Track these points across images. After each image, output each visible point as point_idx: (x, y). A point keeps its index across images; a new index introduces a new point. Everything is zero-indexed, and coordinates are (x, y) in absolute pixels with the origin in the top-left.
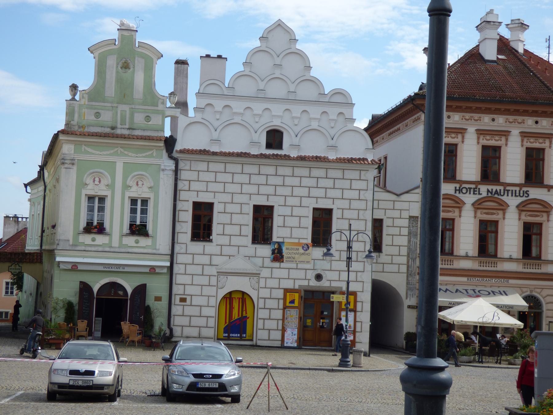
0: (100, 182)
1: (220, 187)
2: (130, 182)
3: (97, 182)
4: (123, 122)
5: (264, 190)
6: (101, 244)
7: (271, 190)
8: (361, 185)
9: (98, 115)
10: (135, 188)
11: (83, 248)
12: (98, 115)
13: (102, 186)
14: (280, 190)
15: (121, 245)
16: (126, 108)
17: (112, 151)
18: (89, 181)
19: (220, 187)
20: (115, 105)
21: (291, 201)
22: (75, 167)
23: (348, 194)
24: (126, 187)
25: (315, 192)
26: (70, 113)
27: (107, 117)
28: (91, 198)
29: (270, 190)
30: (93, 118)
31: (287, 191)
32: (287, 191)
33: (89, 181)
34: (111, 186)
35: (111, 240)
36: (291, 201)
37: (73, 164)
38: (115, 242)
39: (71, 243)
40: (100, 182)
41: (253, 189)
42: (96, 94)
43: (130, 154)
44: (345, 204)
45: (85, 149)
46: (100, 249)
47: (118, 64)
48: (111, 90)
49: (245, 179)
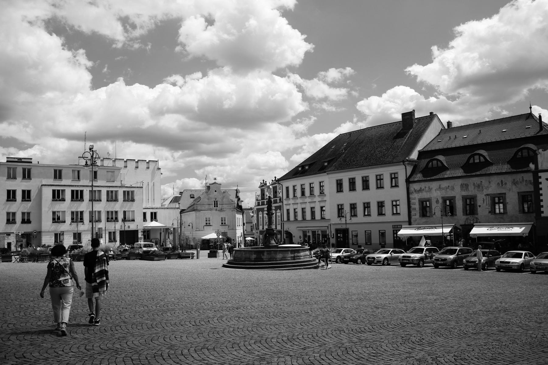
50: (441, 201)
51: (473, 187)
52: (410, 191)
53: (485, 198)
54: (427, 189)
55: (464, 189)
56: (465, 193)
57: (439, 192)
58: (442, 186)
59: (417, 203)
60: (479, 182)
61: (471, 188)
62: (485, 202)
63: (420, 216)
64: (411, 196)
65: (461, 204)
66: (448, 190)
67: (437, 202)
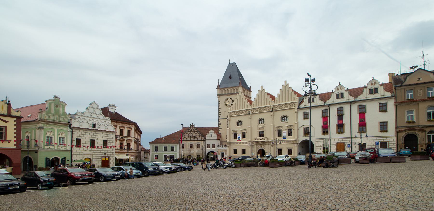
1: (83, 136)
5: (93, 136)
7: (94, 136)
8: (113, 136)
13: (51, 134)
14: (96, 137)
19: (83, 136)
21: (99, 139)
23: (110, 138)
25: (104, 137)
29: (94, 136)
31: (98, 137)
32: (98, 137)
36: (99, 139)
41: (90, 136)
44: (110, 140)
49: (89, 134)
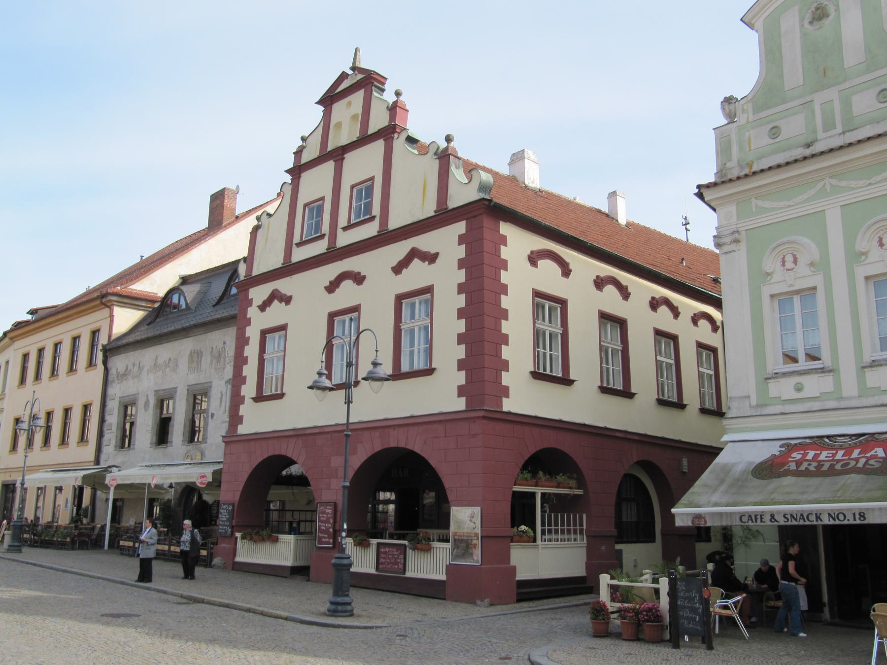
0: (795, 261)
2: (861, 245)
3: (789, 264)
4: (829, 125)
6: (818, 395)
9: (775, 132)
10: (876, 253)
11: (778, 409)
12: (775, 132)
15: (864, 391)
16: (832, 94)
17: (813, 192)
18: (770, 264)
20: (808, 99)
22: (743, 246)
24: (855, 256)
26: (723, 148)
27: (794, 128)
28: (783, 299)
30: (767, 140)
33: (770, 264)
34: (821, 265)
35: (838, 384)
37: (737, 241)
38: (850, 387)
39: (754, 402)
40: (795, 261)
42: (768, 92)
43: (853, 184)
45: (757, 206)
46: (816, 406)
47: (802, 19)
48: (794, 74)
50: (152, 402)
51: (209, 358)
52: (110, 378)
53: (224, 393)
54: (136, 369)
55: (195, 365)
56: (194, 379)
57: (151, 376)
58: (161, 361)
59: (116, 411)
60: (221, 345)
61: (206, 360)
62: (223, 404)
63: (116, 447)
64: (111, 391)
65: (184, 410)
66: (167, 370)
67: (147, 404)
